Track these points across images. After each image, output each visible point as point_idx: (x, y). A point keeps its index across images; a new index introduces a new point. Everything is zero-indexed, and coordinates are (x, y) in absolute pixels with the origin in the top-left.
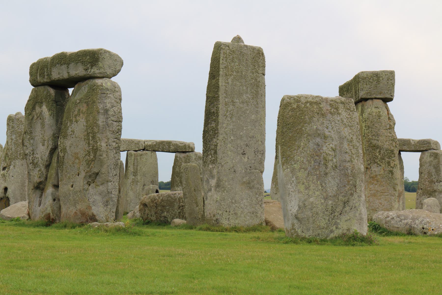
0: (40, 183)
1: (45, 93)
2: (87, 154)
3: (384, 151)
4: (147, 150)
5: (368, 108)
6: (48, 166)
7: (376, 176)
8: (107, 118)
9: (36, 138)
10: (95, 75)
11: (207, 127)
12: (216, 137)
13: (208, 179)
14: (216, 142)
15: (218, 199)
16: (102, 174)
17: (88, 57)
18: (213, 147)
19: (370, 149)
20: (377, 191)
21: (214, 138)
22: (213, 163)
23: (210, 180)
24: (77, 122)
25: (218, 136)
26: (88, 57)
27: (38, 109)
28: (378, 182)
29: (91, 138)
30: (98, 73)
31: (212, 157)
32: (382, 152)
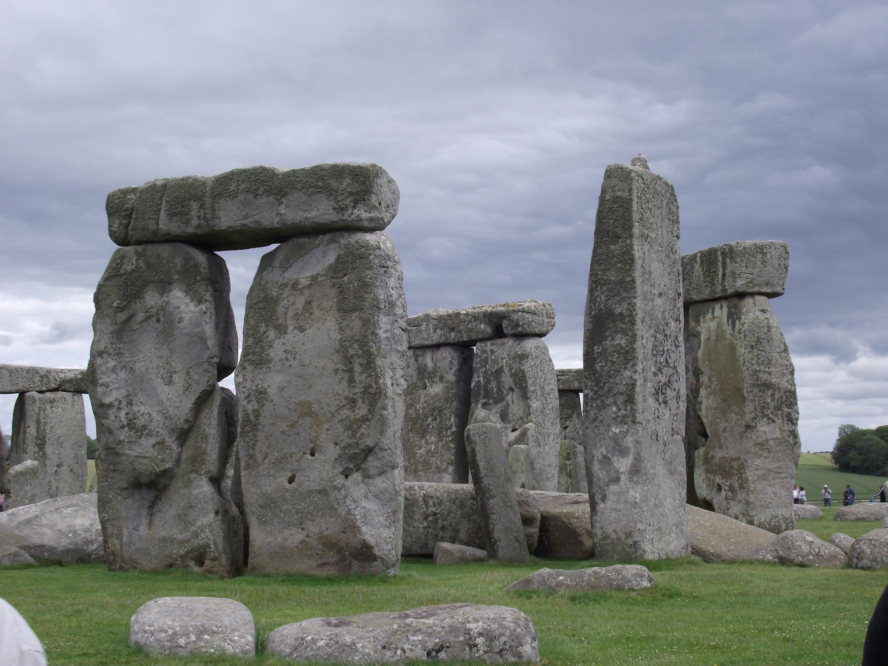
0: (166, 473)
1: (178, 261)
2: (344, 406)
3: (782, 393)
4: (64, 390)
5: (748, 312)
6: (184, 435)
7: (767, 441)
8: (393, 324)
9: (140, 367)
10: (360, 224)
11: (600, 343)
12: (629, 366)
13: (605, 457)
14: (631, 377)
15: (637, 500)
16: (382, 450)
17: (348, 181)
18: (622, 388)
19: (756, 390)
20: (770, 470)
21: (625, 368)
22: (623, 422)
23: (615, 459)
24: (302, 329)
25: (635, 365)
26: (348, 181)
27: (151, 299)
28: (769, 452)
29: (357, 368)
30: (367, 220)
31: (619, 410)
32: (777, 395)
